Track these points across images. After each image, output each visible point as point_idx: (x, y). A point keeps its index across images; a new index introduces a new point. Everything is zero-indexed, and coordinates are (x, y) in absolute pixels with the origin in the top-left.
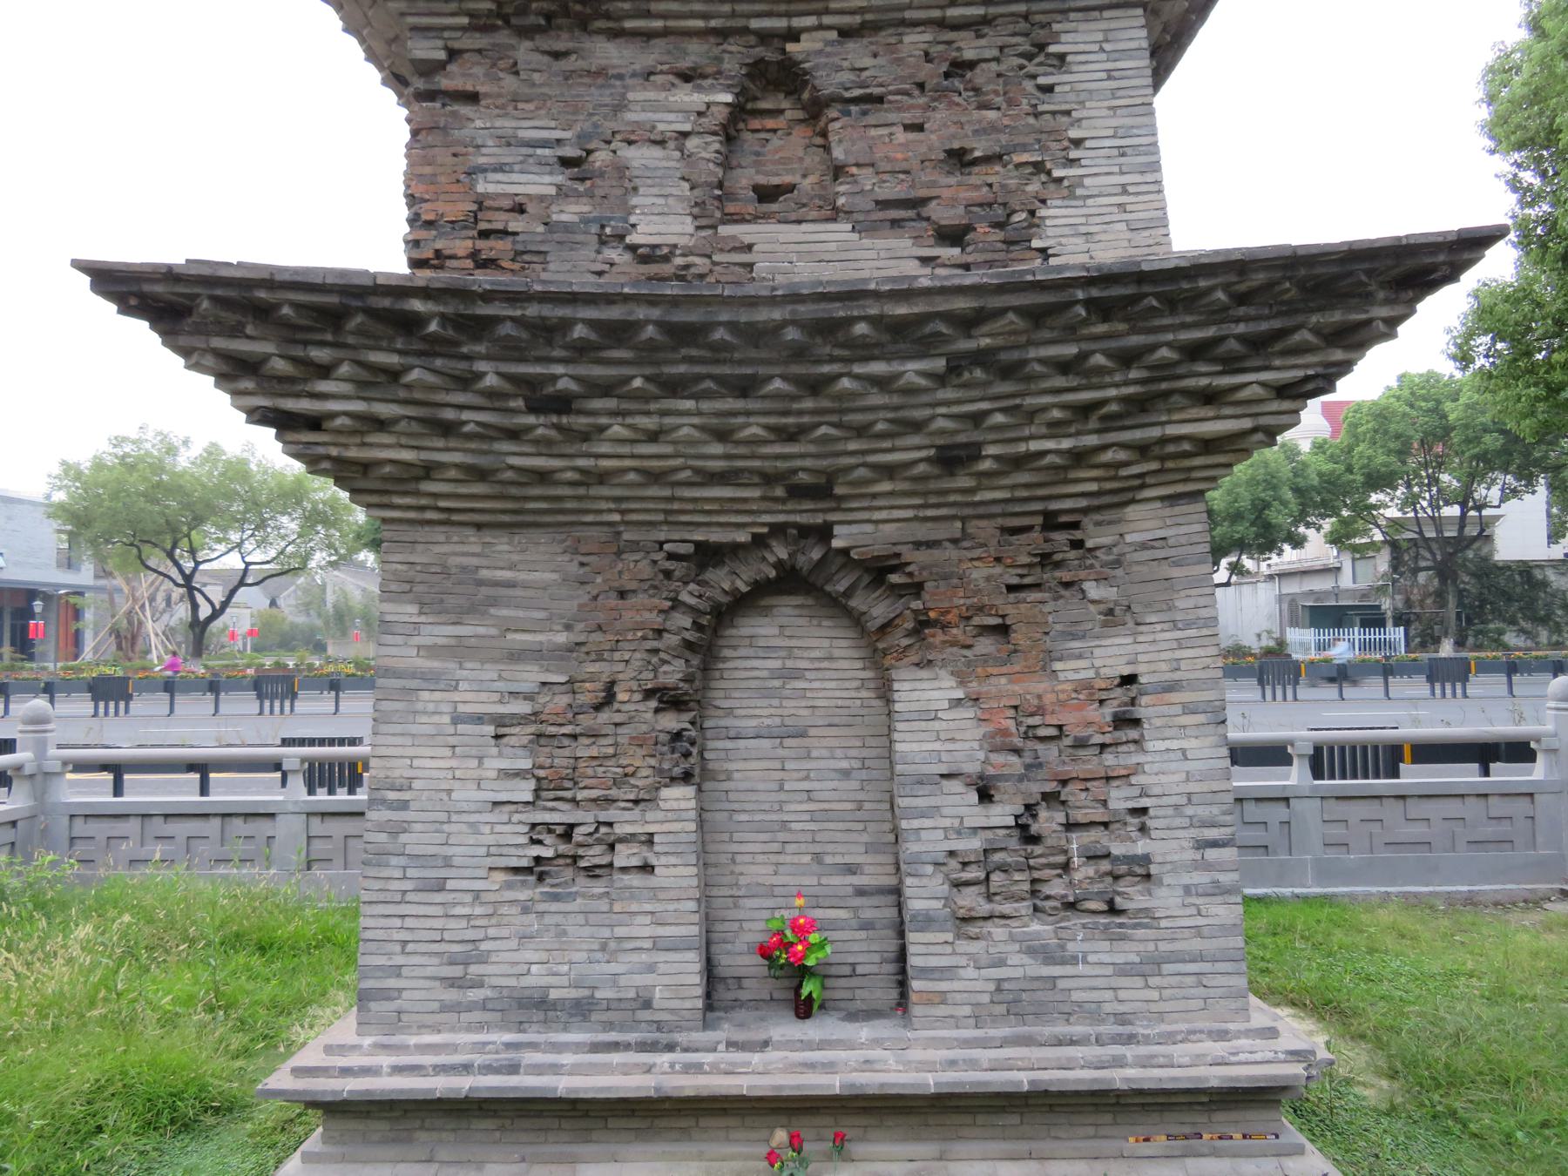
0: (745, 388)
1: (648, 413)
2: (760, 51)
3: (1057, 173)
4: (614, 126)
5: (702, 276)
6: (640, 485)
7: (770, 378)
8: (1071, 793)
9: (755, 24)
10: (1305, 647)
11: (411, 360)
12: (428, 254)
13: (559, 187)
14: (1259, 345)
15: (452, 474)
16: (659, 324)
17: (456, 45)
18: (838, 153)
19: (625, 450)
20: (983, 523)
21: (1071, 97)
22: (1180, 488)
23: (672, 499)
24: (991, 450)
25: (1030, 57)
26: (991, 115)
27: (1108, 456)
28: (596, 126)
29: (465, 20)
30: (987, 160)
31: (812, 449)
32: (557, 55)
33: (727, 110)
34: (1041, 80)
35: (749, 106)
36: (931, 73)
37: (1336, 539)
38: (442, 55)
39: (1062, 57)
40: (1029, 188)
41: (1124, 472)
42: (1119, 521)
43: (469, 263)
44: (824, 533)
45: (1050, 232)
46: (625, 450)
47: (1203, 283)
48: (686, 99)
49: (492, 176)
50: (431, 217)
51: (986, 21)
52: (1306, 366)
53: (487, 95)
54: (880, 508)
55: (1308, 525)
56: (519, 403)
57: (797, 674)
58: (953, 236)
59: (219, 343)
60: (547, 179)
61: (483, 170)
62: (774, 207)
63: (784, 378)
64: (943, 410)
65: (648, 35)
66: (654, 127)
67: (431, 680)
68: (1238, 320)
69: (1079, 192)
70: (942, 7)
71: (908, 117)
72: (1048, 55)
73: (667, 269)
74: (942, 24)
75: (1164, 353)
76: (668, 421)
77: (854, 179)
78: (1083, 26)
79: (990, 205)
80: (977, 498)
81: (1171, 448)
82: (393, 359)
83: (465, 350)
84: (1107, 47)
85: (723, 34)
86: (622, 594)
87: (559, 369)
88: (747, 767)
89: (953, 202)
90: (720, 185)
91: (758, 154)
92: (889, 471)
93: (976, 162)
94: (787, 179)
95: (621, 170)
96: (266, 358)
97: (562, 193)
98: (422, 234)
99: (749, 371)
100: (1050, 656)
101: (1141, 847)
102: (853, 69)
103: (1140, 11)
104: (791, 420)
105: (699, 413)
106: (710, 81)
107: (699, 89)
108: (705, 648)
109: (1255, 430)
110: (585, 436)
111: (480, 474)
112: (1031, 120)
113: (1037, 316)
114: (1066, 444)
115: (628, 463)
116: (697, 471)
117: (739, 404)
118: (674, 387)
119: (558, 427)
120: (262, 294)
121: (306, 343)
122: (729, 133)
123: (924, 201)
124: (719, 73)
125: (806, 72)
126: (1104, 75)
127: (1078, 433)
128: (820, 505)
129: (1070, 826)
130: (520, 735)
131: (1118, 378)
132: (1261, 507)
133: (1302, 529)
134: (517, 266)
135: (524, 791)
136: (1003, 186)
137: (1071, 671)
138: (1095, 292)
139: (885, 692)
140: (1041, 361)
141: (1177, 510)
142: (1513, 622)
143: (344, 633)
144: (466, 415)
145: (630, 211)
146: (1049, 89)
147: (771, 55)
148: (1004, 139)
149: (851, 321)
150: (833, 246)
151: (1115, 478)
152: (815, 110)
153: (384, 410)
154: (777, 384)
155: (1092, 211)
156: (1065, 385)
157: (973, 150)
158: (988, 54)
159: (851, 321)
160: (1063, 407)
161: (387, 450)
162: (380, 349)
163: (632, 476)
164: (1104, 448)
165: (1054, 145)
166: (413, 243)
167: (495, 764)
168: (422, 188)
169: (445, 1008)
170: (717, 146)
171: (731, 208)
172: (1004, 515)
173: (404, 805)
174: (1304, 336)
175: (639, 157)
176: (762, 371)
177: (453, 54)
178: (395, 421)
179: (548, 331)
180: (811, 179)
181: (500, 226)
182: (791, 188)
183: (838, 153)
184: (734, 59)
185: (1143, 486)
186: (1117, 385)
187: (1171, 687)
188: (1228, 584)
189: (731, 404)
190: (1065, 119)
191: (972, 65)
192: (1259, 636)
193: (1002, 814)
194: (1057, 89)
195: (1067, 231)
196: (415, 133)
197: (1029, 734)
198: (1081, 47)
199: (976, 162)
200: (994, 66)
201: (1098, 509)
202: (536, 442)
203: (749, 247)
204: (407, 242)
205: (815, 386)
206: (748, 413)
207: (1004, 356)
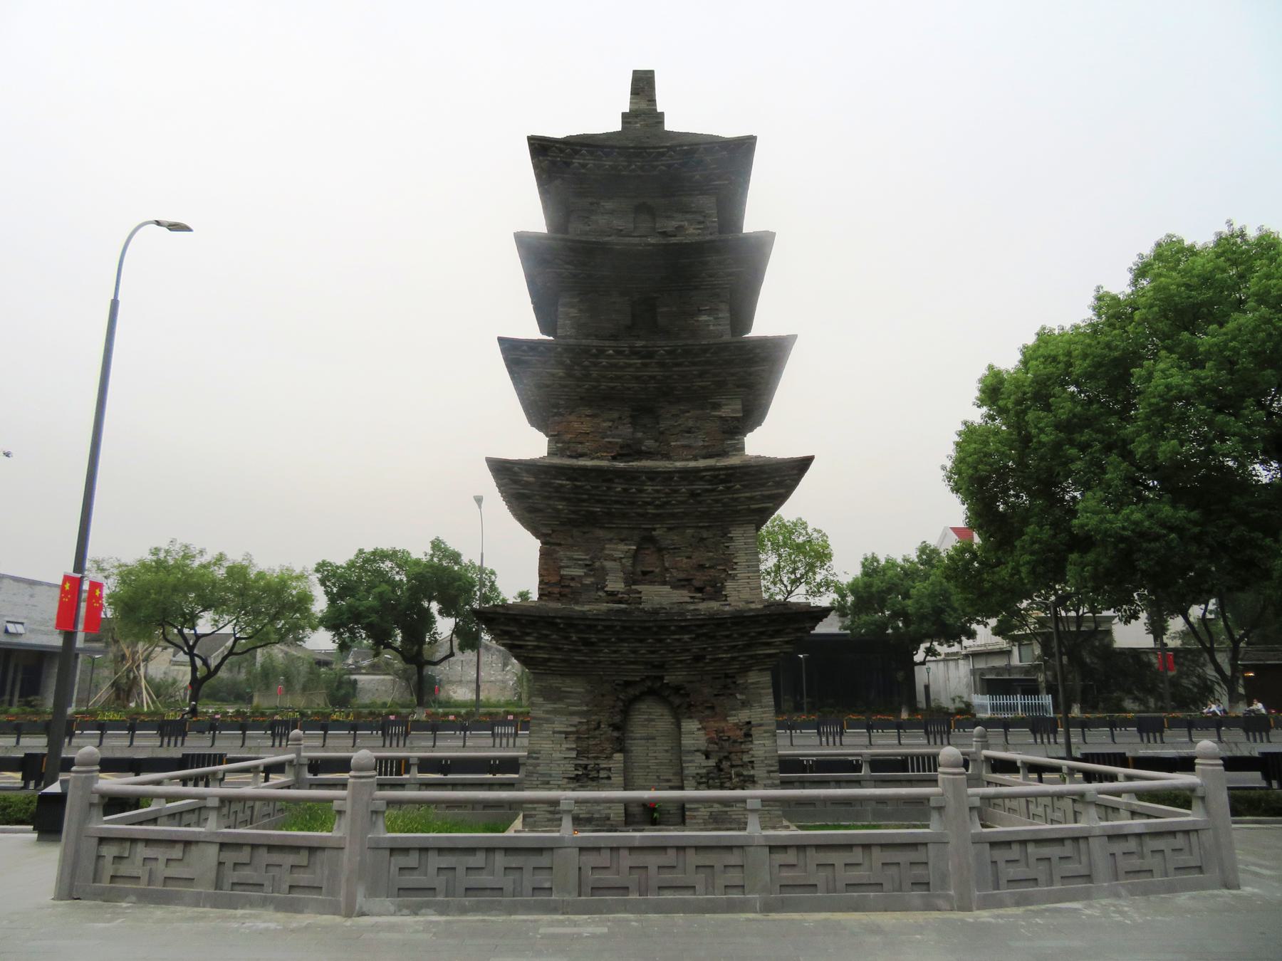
0: (641, 641)
8: (733, 756)
10: (983, 707)
14: (777, 633)
30: (710, 567)
37: (997, 631)
44: (662, 678)
55: (978, 623)
57: (653, 720)
58: (700, 590)
67: (547, 721)
86: (603, 695)
88: (638, 749)
92: (681, 661)
95: (603, 568)
97: (586, 575)
100: (727, 716)
101: (752, 772)
108: (626, 712)
110: (596, 652)
118: (623, 640)
122: (635, 556)
129: (732, 766)
130: (573, 737)
132: (938, 612)
133: (974, 626)
135: (574, 754)
137: (732, 720)
139: (679, 727)
142: (1129, 692)
143: (268, 687)
152: (660, 550)
167: (565, 746)
169: (549, 820)
173: (537, 758)
175: (608, 564)
183: (667, 564)
187: (761, 725)
188: (923, 663)
192: (953, 700)
193: (712, 762)
197: (720, 738)
205: (660, 641)
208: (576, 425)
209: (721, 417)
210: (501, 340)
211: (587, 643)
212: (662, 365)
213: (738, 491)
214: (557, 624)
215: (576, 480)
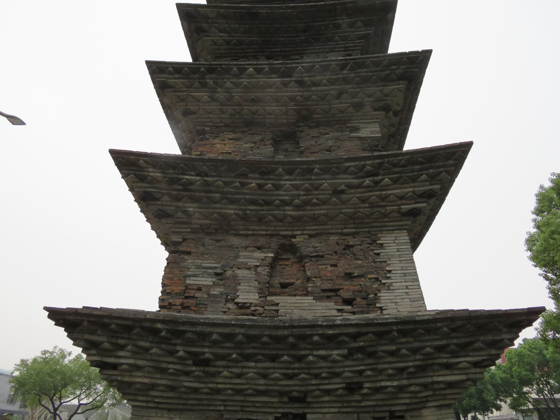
0: (273, 358)
1: (237, 367)
2: (283, 241)
3: (383, 281)
4: (233, 263)
5: (260, 314)
6: (232, 395)
7: (283, 355)
9: (282, 233)
11: (153, 345)
12: (167, 304)
13: (214, 282)
14: (463, 348)
15: (162, 388)
16: (243, 334)
17: (186, 237)
18: (308, 273)
19: (227, 381)
20: (365, 415)
21: (386, 257)
22: (442, 402)
23: (244, 401)
24: (367, 385)
25: (371, 244)
26: (359, 262)
27: (412, 389)
28: (228, 263)
29: (190, 230)
30: (359, 276)
31: (298, 383)
32: (218, 241)
33: (272, 259)
34: (375, 252)
35: (279, 257)
36: (340, 248)
38: (181, 240)
39: (382, 245)
40: (374, 286)
41: (419, 395)
42: (420, 416)
43: (180, 307)
45: (382, 301)
46: (227, 381)
47: (439, 325)
48: (258, 255)
49: (192, 278)
50: (169, 291)
51: (356, 233)
52: (483, 356)
53: (193, 253)
54: (325, 407)
55: (501, 400)
56: (190, 362)
58: (348, 302)
59: (87, 336)
60: (210, 279)
61: (189, 276)
62: (287, 290)
63: (288, 355)
64: (347, 369)
65: (247, 236)
66: (247, 264)
68: (454, 338)
69: (391, 288)
70: (342, 229)
71: (332, 262)
72: (377, 244)
73: (248, 311)
74: (342, 234)
75: (428, 350)
76: (244, 370)
77: (314, 282)
78: (387, 235)
79: (361, 292)
80: (363, 404)
81: (436, 386)
82: (148, 344)
83: (173, 342)
84: (396, 241)
85: (271, 236)
87: (206, 350)
89: (348, 290)
90: (268, 283)
91: (281, 272)
92: (328, 392)
93: (355, 277)
94: (291, 281)
95: (235, 277)
96: (102, 342)
97: (215, 285)
98: (165, 297)
99: (275, 352)
102: (314, 247)
103: (406, 231)
104: (290, 371)
105: (256, 368)
106: (266, 250)
107: (263, 252)
109: (468, 380)
110: (214, 375)
111: (172, 389)
112: (373, 264)
113: (380, 335)
114: (395, 383)
115: (228, 386)
116: (254, 390)
117: (271, 365)
118: (247, 358)
119: (204, 372)
120: (106, 320)
121: (117, 337)
122: (272, 265)
123: (338, 290)
124: (269, 248)
125: (298, 248)
126: (396, 250)
127: (400, 379)
128: (301, 405)
131: (412, 358)
133: (498, 402)
134: (196, 309)
136: (365, 285)
138: (400, 327)
140: (383, 351)
141: (443, 412)
144: (170, 366)
145: (237, 291)
146: (378, 254)
147: (287, 242)
148: (364, 270)
149: (312, 335)
150: (307, 305)
151: (416, 397)
152: (301, 259)
153: (140, 363)
154: (285, 358)
155: (397, 294)
156: (394, 361)
157: (354, 273)
158: (357, 243)
159: (312, 335)
160: (393, 369)
161: (140, 379)
162: (143, 340)
163: (230, 392)
164: (411, 385)
165: (381, 272)
166: (161, 300)
168: (168, 281)
170: (268, 270)
171: (271, 290)
172: (374, 412)
174: (479, 344)
175: (241, 273)
176: (280, 352)
177: (184, 240)
178: (144, 367)
179: (203, 336)
180: (299, 281)
181: (192, 295)
182: (292, 284)
183: (308, 273)
184: (275, 243)
185: (428, 401)
186: (412, 361)
189: (268, 364)
190: (384, 264)
191: (352, 246)
194: (381, 254)
195: (389, 301)
196: (168, 264)
198: (388, 242)
199: (355, 277)
200: (359, 247)
201: (411, 410)
202: (195, 377)
203: (277, 304)
204: (160, 299)
205: (300, 359)
206: (274, 368)
207: (369, 349)
208: (218, 146)
209: (360, 138)
210: (150, 64)
211: (200, 361)
212: (301, 83)
213: (386, 187)
214: (159, 331)
215: (207, 176)
